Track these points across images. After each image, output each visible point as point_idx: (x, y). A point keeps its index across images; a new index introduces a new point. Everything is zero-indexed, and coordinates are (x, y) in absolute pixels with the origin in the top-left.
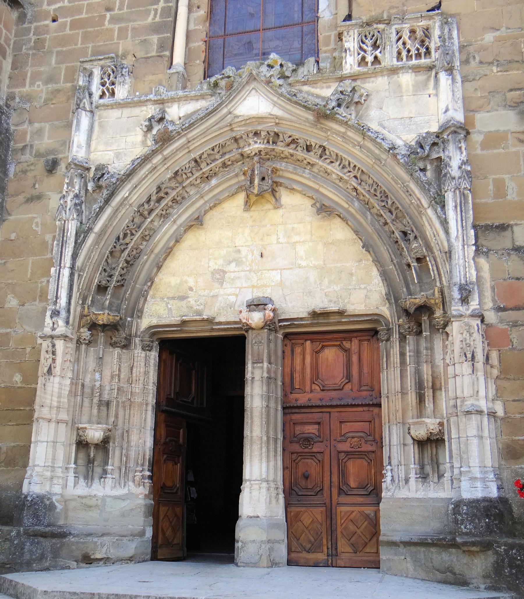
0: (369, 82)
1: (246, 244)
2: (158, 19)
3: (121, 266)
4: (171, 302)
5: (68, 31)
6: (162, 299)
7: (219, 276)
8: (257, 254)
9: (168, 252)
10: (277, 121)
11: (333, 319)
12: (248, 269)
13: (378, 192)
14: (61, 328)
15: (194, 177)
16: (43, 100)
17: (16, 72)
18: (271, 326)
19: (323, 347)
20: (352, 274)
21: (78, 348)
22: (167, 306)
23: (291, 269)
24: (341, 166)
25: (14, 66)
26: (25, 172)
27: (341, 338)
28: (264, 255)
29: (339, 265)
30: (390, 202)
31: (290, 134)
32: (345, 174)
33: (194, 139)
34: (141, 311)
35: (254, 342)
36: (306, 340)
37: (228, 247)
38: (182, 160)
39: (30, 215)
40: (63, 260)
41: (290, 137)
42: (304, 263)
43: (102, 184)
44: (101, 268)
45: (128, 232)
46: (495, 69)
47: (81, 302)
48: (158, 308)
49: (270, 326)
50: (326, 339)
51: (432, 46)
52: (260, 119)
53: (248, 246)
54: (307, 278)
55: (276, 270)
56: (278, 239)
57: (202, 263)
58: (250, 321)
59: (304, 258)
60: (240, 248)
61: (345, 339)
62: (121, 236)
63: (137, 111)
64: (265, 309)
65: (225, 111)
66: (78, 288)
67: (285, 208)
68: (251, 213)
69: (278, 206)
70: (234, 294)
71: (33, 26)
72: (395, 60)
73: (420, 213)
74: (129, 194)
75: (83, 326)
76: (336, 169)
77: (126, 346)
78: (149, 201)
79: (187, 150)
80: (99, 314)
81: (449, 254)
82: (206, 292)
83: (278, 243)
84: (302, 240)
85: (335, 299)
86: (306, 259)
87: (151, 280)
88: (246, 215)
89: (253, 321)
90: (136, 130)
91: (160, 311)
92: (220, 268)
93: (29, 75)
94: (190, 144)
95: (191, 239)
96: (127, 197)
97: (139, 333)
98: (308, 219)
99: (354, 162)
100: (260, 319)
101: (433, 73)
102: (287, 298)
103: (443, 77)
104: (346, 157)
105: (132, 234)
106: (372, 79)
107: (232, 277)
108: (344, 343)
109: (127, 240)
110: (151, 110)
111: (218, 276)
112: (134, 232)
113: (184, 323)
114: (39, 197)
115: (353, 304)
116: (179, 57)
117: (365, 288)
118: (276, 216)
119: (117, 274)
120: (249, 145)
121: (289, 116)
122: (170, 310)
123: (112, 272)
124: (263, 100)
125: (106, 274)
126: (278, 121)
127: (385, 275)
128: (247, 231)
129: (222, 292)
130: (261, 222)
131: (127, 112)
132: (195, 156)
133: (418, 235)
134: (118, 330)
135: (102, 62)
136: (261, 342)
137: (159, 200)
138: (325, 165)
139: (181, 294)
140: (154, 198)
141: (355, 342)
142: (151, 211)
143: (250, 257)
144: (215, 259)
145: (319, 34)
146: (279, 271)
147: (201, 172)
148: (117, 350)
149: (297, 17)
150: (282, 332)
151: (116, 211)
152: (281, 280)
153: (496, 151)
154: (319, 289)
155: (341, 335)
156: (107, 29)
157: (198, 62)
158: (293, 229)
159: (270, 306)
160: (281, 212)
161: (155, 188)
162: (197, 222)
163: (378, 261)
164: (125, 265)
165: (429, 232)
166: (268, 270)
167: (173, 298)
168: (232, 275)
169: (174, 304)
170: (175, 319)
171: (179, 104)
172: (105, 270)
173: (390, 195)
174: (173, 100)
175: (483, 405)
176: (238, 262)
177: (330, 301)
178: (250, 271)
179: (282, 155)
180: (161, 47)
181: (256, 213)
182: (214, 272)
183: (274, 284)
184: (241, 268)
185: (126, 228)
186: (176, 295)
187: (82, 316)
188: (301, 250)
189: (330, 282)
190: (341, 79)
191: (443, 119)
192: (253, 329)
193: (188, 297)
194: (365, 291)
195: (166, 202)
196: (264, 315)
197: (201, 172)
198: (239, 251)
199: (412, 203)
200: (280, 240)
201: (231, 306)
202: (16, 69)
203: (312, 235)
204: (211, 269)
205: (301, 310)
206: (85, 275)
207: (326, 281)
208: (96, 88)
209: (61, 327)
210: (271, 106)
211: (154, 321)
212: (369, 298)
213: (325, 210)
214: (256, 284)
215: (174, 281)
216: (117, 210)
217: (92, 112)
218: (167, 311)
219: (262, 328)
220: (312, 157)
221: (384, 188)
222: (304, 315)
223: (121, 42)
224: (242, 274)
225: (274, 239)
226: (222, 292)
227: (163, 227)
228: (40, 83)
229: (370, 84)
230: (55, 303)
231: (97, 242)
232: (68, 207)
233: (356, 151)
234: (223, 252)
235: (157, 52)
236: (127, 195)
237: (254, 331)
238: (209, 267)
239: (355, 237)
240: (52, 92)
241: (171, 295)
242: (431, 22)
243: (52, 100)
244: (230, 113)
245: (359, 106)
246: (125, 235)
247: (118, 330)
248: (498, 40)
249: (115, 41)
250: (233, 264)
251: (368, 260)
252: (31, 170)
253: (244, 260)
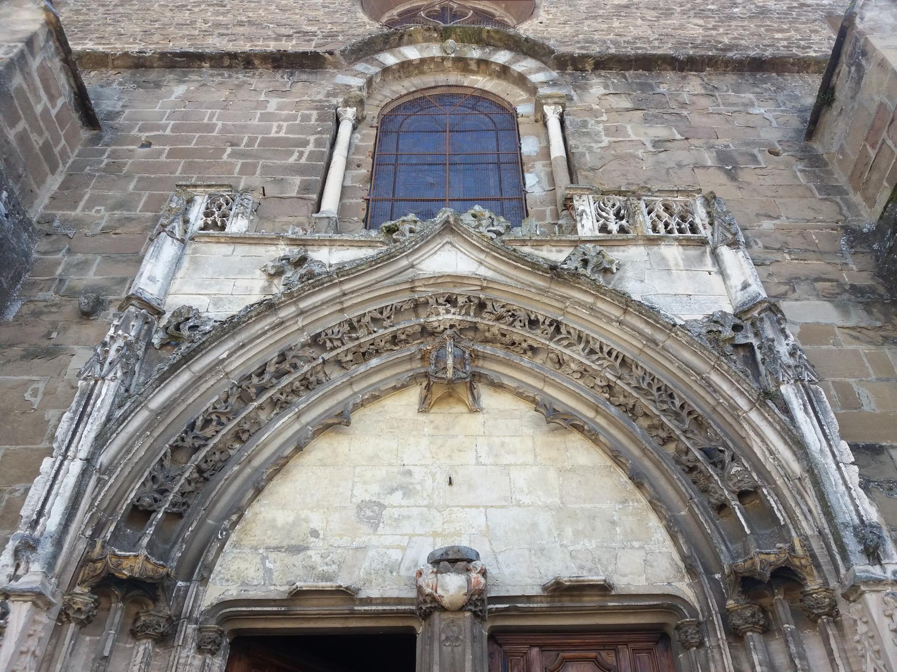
0: (618, 251)
1: (423, 462)
2: (303, 161)
3: (187, 475)
4: (273, 556)
5: (163, 158)
6: (255, 548)
8: (442, 480)
9: (280, 465)
10: (485, 285)
11: (591, 601)
12: (425, 503)
13: (655, 388)
15: (345, 348)
16: (100, 228)
17: (66, 192)
19: (565, 660)
20: (613, 523)
21: (57, 632)
22: (264, 564)
23: (503, 507)
24: (586, 351)
25: (64, 186)
26: (37, 314)
27: (598, 644)
28: (454, 481)
29: (588, 506)
30: (678, 403)
31: (504, 302)
32: (593, 362)
33: (352, 292)
34: (210, 568)
35: (443, 637)
36: (532, 646)
37: (391, 465)
38: (330, 321)
39: (26, 378)
40: (73, 445)
41: (503, 306)
42: (526, 500)
43: (180, 338)
44: (146, 474)
45: (214, 417)
46: (787, 257)
47: (89, 533)
48: (243, 566)
49: (476, 606)
50: (570, 645)
51: (698, 221)
52: (458, 279)
53: (426, 466)
54: (534, 525)
55: (477, 507)
56: (478, 457)
57: (341, 490)
58: (440, 592)
59: (526, 490)
60: (412, 468)
61: (605, 646)
62: (199, 423)
63: (260, 250)
64: (468, 570)
65: (404, 263)
66: (92, 505)
67: (488, 412)
68: (431, 417)
69: (475, 408)
70: (398, 547)
71: (109, 149)
72: (650, 230)
73: (737, 418)
74: (229, 356)
75: (83, 582)
76: (579, 354)
77: (165, 640)
78: (261, 373)
79: (338, 307)
80: (127, 557)
82: (345, 541)
83: (479, 464)
84: (519, 462)
85: (589, 565)
86: (530, 492)
87: (238, 510)
88: (422, 418)
89: (448, 591)
90: (254, 273)
92: (374, 499)
93: (86, 197)
94: (346, 298)
95: (323, 448)
96: (224, 360)
97: (196, 614)
98: (528, 431)
99: (609, 344)
100: (461, 587)
101: (708, 249)
102: (500, 558)
103: (726, 252)
104: (596, 336)
105: (220, 423)
106: (623, 248)
107: (396, 516)
108: (604, 654)
109: (209, 431)
110: (282, 250)
111: (369, 513)
112: (224, 419)
113: (298, 594)
114: (51, 353)
115: (625, 576)
117: (641, 548)
118: (474, 422)
119: (177, 488)
120: (438, 314)
121: (503, 279)
122: (269, 571)
123: (168, 485)
124: (464, 256)
125: (155, 487)
126: (485, 284)
127: (673, 528)
128: (425, 442)
129: (374, 540)
130: (447, 429)
131: (241, 250)
132: (351, 317)
133: (738, 453)
134: (155, 600)
135: (212, 190)
136: (457, 639)
137: (279, 375)
138: (560, 348)
139: (293, 542)
140: (271, 369)
141: (625, 654)
142: (262, 390)
143: (429, 483)
144: (365, 483)
145: (529, 208)
146: (483, 510)
147: (357, 343)
148: (144, 646)
150: (488, 625)
151: (199, 379)
152: (487, 526)
153: (824, 347)
154: (558, 545)
155: (601, 638)
156: (225, 162)
157: (356, 219)
158: (503, 445)
159: (478, 564)
160: (480, 417)
161: (277, 354)
162: (338, 422)
163: (657, 503)
164: (196, 475)
165: (758, 448)
166: (463, 507)
167: (278, 549)
168: (396, 513)
170: (279, 589)
171: (331, 249)
172: (154, 479)
173: (676, 392)
174: (320, 243)
176: (408, 491)
177: (582, 567)
178: (428, 507)
179: (487, 334)
180: (306, 188)
182: (361, 507)
183: (473, 531)
184: (412, 501)
185: (211, 410)
186: (285, 544)
187: (86, 560)
188: (520, 478)
189: (576, 533)
190: (576, 243)
191: (741, 297)
192: (443, 609)
193: (307, 548)
194: (642, 553)
195: (291, 379)
196: (469, 581)
197: (357, 343)
198: (409, 473)
199: (719, 403)
200: (482, 460)
201: (393, 568)
202: (68, 188)
203: (535, 456)
204: (357, 500)
205: (529, 581)
206: (112, 481)
207: (569, 531)
208: (196, 215)
209: (35, 573)
210: (476, 265)
211: (233, 592)
212: (651, 566)
214: (440, 530)
215: (283, 517)
216: (200, 378)
217: (182, 241)
218: (261, 573)
219: (462, 609)
220: (537, 338)
221: (666, 382)
222: (536, 591)
223: (244, 177)
224: (415, 511)
225: (470, 457)
226: (374, 540)
227: (278, 420)
228: (103, 208)
229: (620, 253)
230: (34, 524)
231: (150, 425)
232: (109, 360)
233: (614, 329)
234: (381, 473)
235: (298, 192)
236: (224, 356)
237: (446, 616)
238: (352, 496)
239: (609, 462)
240: (119, 220)
241: (274, 543)
242: (690, 199)
243: (116, 228)
244: (413, 266)
245: (609, 275)
246: (207, 422)
247: (155, 600)
248: (779, 228)
249: (236, 175)
250: (399, 494)
251: (640, 501)
252: (51, 312)
253: (418, 487)
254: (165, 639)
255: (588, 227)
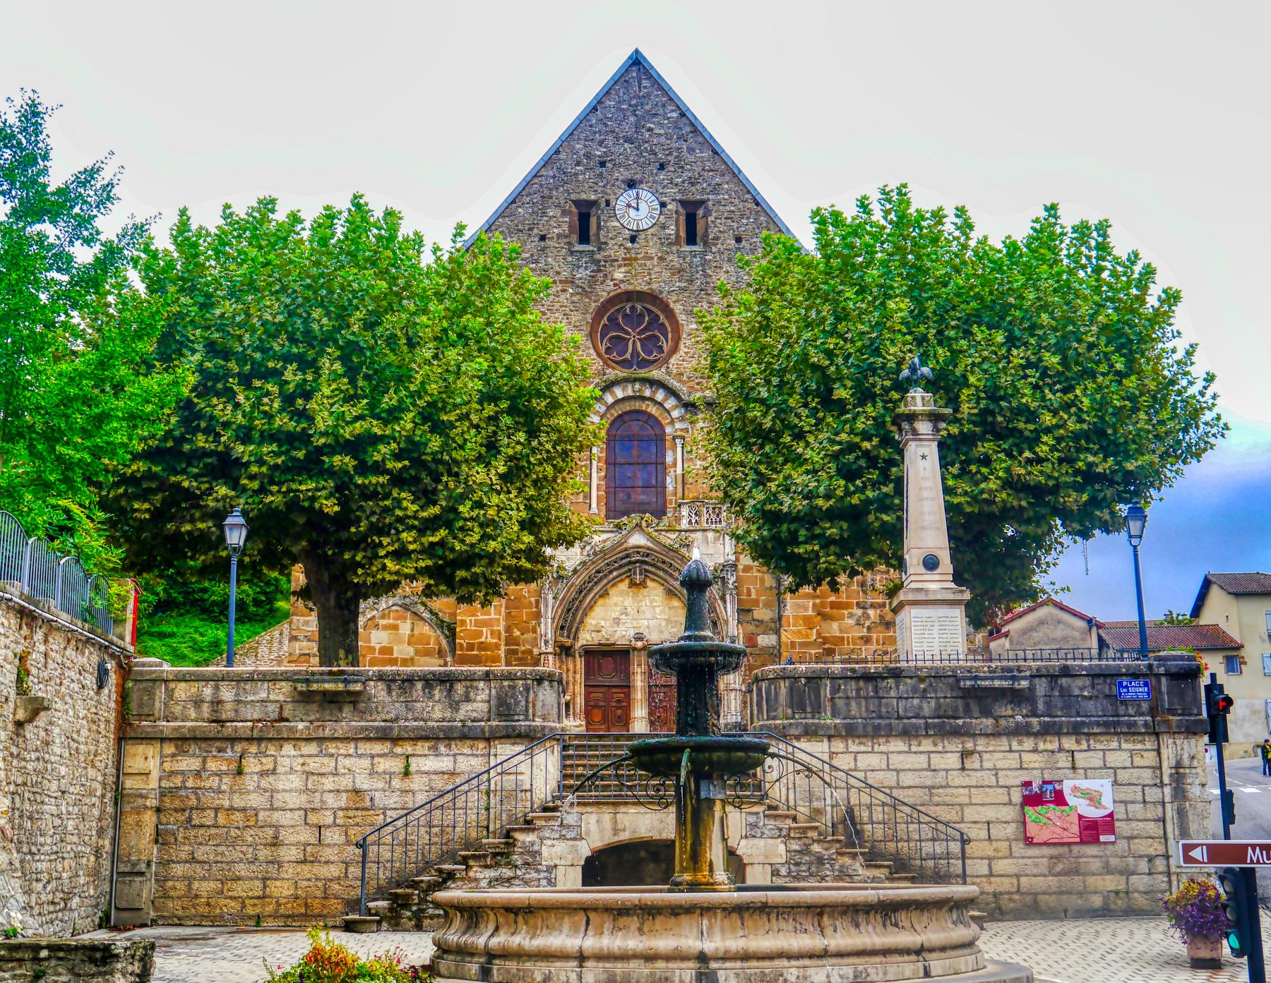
7: (617, 621)
14: (550, 649)
18: (644, 648)
81: (726, 622)
87: (582, 622)
91: (586, 637)
116: (594, 505)
118: (645, 591)
126: (649, 549)
149: (654, 482)
162: (604, 594)
169: (594, 635)
170: (596, 642)
175: (737, 687)
181: (634, 589)
188: (658, 610)
213: (670, 593)
215: (594, 622)
220: (664, 566)
254: (574, 657)
255: (684, 524)
